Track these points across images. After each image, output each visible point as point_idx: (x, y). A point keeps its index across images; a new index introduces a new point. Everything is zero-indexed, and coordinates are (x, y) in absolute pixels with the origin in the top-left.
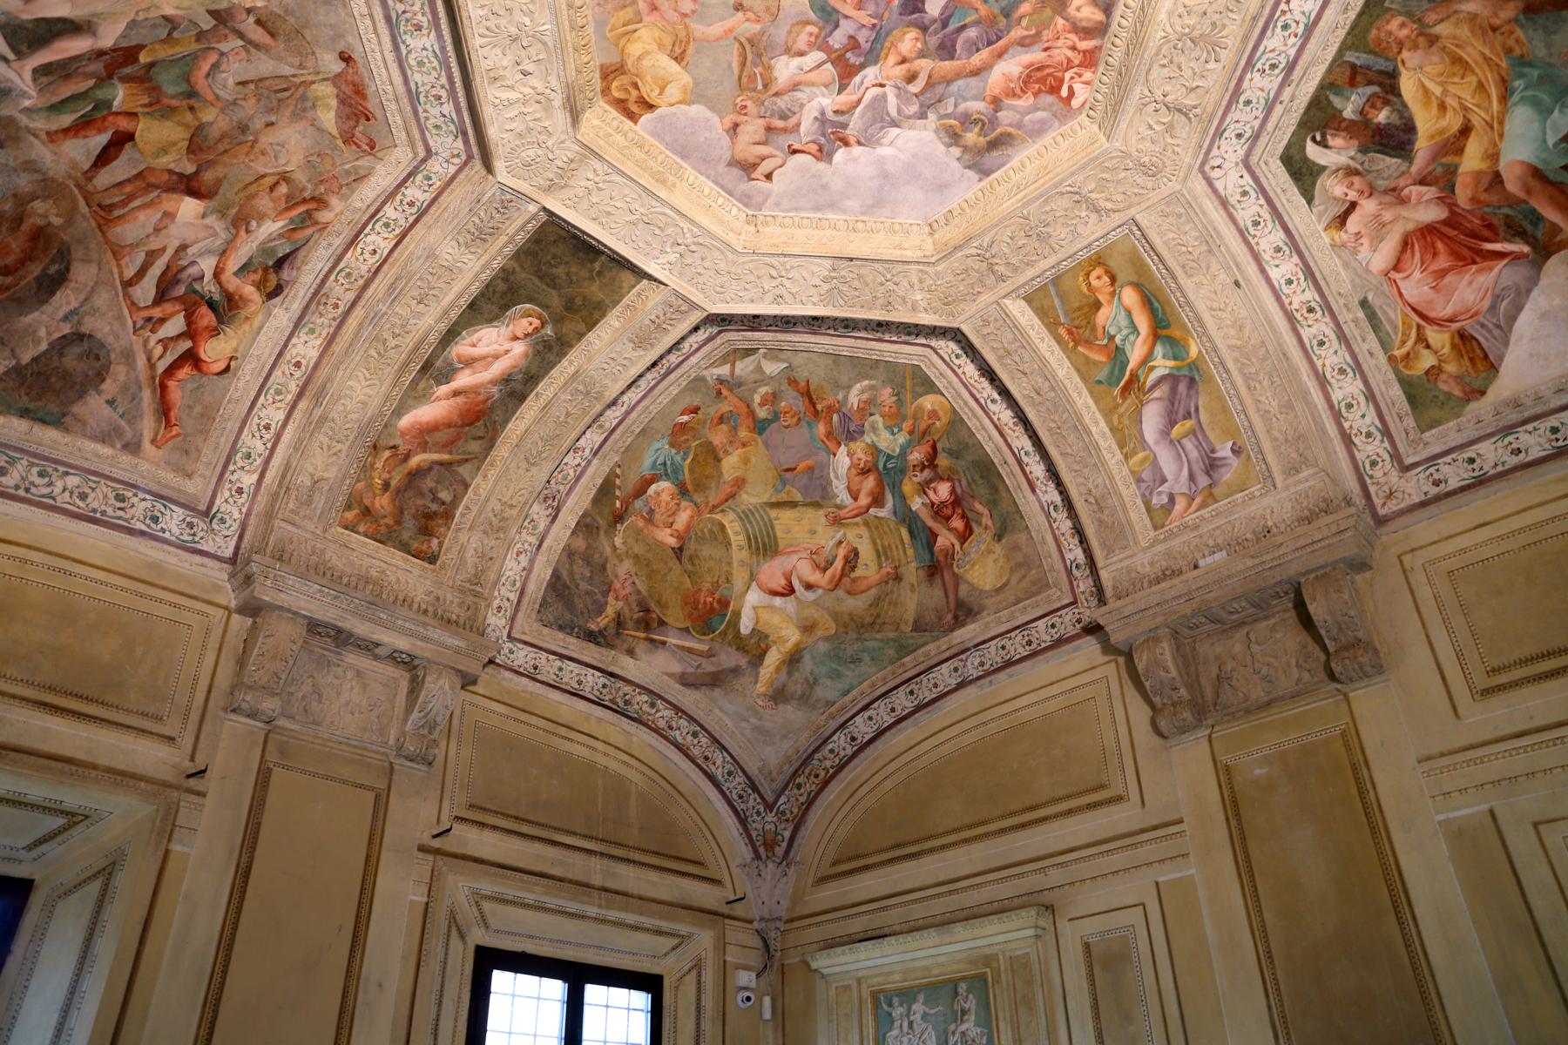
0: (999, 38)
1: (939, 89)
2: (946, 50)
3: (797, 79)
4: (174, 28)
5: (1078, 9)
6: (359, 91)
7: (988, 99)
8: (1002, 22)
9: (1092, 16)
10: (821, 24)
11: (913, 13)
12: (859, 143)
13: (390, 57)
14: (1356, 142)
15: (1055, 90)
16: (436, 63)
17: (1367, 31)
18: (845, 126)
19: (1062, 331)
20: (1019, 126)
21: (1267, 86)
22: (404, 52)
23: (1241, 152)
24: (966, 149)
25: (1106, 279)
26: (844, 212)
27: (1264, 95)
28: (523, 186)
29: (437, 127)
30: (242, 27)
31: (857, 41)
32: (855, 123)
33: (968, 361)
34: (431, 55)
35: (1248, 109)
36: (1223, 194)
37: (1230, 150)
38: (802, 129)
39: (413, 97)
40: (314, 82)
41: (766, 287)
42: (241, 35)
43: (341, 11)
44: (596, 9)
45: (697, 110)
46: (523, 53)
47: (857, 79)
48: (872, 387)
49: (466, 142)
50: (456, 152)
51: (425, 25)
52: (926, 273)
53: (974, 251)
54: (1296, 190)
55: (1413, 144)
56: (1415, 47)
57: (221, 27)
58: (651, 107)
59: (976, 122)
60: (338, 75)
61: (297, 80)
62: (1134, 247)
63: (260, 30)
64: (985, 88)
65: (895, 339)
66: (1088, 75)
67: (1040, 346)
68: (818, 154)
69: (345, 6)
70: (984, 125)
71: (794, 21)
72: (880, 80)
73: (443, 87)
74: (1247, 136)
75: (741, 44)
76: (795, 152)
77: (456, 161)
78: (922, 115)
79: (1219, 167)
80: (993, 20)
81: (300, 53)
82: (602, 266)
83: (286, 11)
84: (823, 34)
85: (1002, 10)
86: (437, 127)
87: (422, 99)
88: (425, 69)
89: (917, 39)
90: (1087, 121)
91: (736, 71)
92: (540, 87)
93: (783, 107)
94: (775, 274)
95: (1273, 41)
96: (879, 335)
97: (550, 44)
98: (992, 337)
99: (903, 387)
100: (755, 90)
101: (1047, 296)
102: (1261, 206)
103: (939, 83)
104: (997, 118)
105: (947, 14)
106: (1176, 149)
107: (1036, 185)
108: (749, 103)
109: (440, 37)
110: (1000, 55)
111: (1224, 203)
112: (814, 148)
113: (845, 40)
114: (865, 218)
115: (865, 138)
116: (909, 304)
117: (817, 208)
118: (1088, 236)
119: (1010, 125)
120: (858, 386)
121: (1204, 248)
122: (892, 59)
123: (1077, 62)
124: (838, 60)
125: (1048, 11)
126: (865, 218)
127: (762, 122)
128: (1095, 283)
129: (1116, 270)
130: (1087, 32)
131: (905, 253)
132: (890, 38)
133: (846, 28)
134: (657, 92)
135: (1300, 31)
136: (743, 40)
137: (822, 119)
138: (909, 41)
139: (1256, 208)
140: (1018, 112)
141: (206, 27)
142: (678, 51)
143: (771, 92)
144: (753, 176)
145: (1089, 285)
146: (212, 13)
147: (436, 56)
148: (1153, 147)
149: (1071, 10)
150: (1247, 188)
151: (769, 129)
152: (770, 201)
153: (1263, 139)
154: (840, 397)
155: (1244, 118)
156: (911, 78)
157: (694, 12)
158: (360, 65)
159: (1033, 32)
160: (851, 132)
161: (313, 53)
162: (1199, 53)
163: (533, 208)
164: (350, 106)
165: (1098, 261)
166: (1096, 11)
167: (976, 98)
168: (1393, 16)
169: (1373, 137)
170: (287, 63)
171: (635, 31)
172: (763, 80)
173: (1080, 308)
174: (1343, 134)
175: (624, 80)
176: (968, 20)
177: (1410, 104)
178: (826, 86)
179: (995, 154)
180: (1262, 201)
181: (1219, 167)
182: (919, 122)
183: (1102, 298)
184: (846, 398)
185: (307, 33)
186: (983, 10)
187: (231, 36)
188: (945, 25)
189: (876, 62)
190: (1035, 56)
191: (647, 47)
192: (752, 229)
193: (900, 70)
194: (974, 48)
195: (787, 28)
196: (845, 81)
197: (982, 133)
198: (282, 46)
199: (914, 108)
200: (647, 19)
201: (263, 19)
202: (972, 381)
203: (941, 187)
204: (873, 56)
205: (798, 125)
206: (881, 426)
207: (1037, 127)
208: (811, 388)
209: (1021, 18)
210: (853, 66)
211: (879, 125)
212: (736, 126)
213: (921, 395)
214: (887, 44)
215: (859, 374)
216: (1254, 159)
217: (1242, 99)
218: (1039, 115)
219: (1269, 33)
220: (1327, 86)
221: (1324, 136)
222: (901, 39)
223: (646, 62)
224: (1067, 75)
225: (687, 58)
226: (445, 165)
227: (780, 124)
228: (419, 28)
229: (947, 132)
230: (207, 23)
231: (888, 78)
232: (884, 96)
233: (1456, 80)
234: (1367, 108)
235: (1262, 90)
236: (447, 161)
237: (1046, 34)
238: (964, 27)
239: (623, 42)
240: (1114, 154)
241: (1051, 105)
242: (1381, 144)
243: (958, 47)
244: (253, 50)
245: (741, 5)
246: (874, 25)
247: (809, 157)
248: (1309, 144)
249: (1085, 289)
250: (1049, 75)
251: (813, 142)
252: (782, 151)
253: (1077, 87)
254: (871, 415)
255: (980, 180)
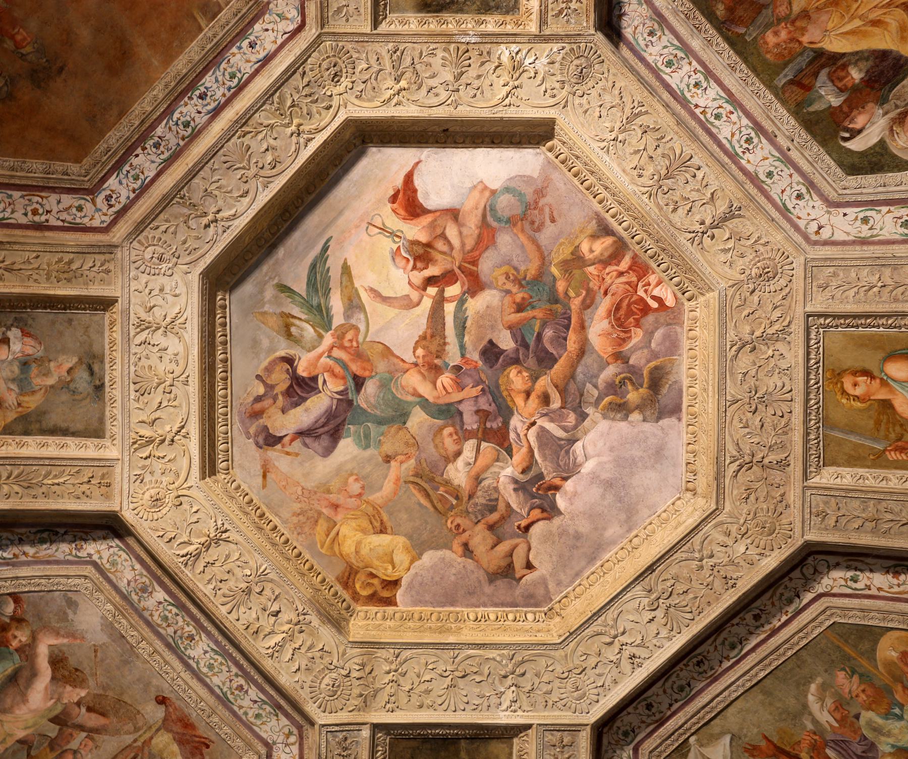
0: (569, 319)
1: (572, 387)
2: (546, 360)
3: (473, 473)
4: (30, 748)
5: (591, 251)
6: (187, 724)
7: (610, 360)
8: (559, 308)
9: (604, 245)
10: (450, 422)
11: (498, 359)
12: (565, 479)
13: (187, 676)
14: (870, 105)
15: (646, 310)
16: (220, 659)
17: (765, 61)
18: (540, 476)
19: (893, 456)
20: (655, 355)
21: (766, 153)
22: (195, 665)
23: (818, 203)
24: (640, 408)
25: (861, 379)
26: (614, 543)
27: (771, 160)
28: (343, 717)
29: (258, 716)
30: (79, 720)
31: (484, 411)
32: (544, 465)
33: (868, 574)
34: (212, 654)
35: (776, 177)
36: (851, 238)
37: (810, 210)
38: (514, 506)
39: (224, 701)
40: (151, 738)
41: (614, 658)
42: (81, 728)
43: (139, 664)
44: (300, 539)
45: (429, 558)
46: (263, 599)
47: (512, 435)
48: (823, 687)
49: (287, 715)
50: (286, 731)
51: (194, 632)
52: (722, 523)
53: (734, 467)
54: (891, 174)
55: (901, 56)
56: (803, 30)
57: (65, 729)
58: (396, 583)
59: (622, 383)
60: (165, 720)
61: (139, 744)
62: (844, 334)
63: (93, 716)
64: (599, 356)
65: (784, 618)
66: (653, 279)
67: (891, 484)
68: (545, 515)
69: (138, 657)
70: (630, 380)
71: (431, 436)
72: (528, 422)
73: (237, 675)
74: (804, 191)
75: (413, 483)
76: (527, 528)
77: (293, 739)
78: (583, 416)
79: (820, 228)
80: (552, 313)
81: (130, 719)
82: (468, 753)
83: (104, 688)
84: (458, 428)
85: (549, 301)
86: (258, 716)
87: (231, 697)
88: (216, 670)
89: (520, 372)
90: (692, 303)
91: (429, 505)
92: (293, 616)
93: (484, 502)
94: (608, 640)
95: (724, 131)
96: (767, 627)
97: (276, 578)
98: (843, 521)
99: (849, 658)
100: (452, 507)
101: (840, 443)
102: (889, 212)
103: (567, 384)
104: (633, 366)
105: (519, 339)
106: (762, 241)
107: (711, 372)
108: (458, 520)
109: (209, 634)
110: (583, 327)
111: (864, 242)
112: (536, 513)
113: (476, 418)
114: (634, 533)
115: (564, 471)
116: (742, 563)
117: (592, 559)
118: (797, 364)
119: (649, 361)
120: (811, 698)
121: (887, 272)
122: (519, 400)
123: (634, 279)
124: (485, 435)
125: (577, 272)
126: (634, 533)
127: (480, 527)
128: (858, 391)
129: (858, 365)
130: (615, 256)
131: (687, 524)
132: (502, 388)
133: (467, 410)
134: (390, 567)
135: (729, 108)
136: (412, 479)
137: (519, 487)
138: (516, 378)
139: (889, 218)
140: (642, 348)
141: (53, 735)
142: (377, 524)
143: (465, 499)
144: (518, 576)
145: (856, 398)
146: (52, 720)
147: (216, 652)
148: (747, 260)
149: (589, 256)
150: (861, 215)
151: (491, 527)
152: (551, 586)
153: (817, 179)
154: (810, 726)
155: (784, 184)
156: (545, 399)
157: (363, 488)
158: (174, 700)
159: (584, 292)
160: (550, 476)
161: (139, 712)
162: (683, 178)
163: (366, 733)
164: (188, 742)
165: (837, 375)
166: (603, 240)
167: (602, 368)
168: (763, 38)
169: (872, 88)
170: (126, 733)
171: (338, 534)
172: (451, 495)
173: (878, 423)
174: (855, 112)
175: (361, 578)
176: (537, 329)
177: (856, 49)
178: (497, 460)
179: (664, 391)
180: (885, 209)
181: (820, 228)
182: (587, 423)
183: (882, 395)
184: (815, 721)
185: (126, 698)
186: (538, 313)
187: (75, 733)
188: (526, 346)
189: (512, 414)
190: (604, 305)
191: (355, 539)
192: (557, 619)
193: (533, 402)
194: (561, 340)
195: (431, 446)
196: (506, 445)
197: (637, 386)
198: (115, 720)
199: (572, 418)
200: (339, 518)
201: (91, 705)
202: (896, 589)
203: (659, 453)
204: (506, 412)
205: (508, 505)
206: (879, 721)
207: (667, 344)
208: (775, 740)
209: (566, 294)
210: (499, 429)
211: (563, 452)
212: (466, 545)
213: (874, 650)
214: (505, 394)
215: (798, 685)
216: (833, 196)
217: (762, 177)
218: (658, 335)
219: (714, 130)
220: (798, 111)
221: (847, 130)
222: (509, 381)
223: (364, 551)
224: (641, 293)
225: (388, 524)
226: (287, 750)
227: (494, 517)
228: (191, 638)
229: (612, 410)
230: (53, 731)
231: (532, 415)
232: (542, 428)
233: (855, 6)
234: (840, 85)
235: (765, 159)
236: (287, 745)
237: (594, 285)
238: (539, 337)
239: (336, 548)
240: (730, 293)
241: (657, 321)
242: (885, 84)
243: (551, 350)
244: (95, 736)
245: (387, 456)
246: (483, 390)
247: (541, 523)
248: (848, 145)
249: (858, 405)
250: (629, 305)
251: (531, 509)
252: (518, 536)
253: (656, 292)
254: (857, 717)
255: (680, 420)
